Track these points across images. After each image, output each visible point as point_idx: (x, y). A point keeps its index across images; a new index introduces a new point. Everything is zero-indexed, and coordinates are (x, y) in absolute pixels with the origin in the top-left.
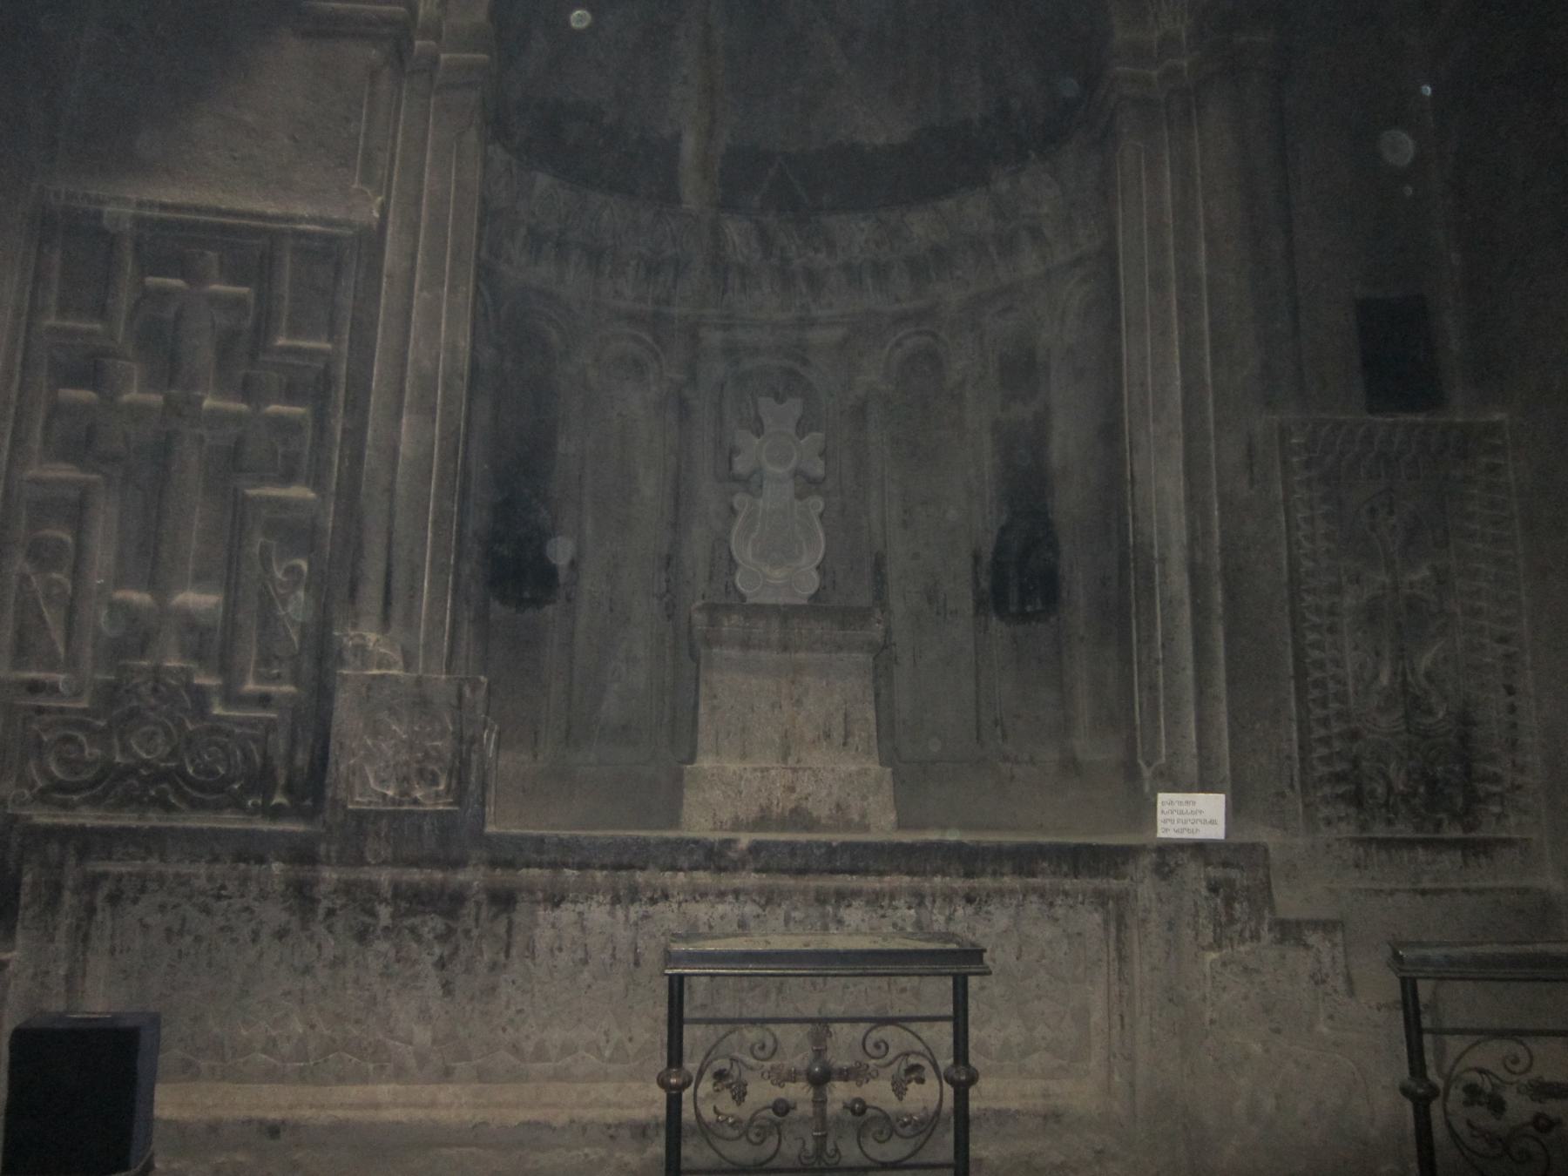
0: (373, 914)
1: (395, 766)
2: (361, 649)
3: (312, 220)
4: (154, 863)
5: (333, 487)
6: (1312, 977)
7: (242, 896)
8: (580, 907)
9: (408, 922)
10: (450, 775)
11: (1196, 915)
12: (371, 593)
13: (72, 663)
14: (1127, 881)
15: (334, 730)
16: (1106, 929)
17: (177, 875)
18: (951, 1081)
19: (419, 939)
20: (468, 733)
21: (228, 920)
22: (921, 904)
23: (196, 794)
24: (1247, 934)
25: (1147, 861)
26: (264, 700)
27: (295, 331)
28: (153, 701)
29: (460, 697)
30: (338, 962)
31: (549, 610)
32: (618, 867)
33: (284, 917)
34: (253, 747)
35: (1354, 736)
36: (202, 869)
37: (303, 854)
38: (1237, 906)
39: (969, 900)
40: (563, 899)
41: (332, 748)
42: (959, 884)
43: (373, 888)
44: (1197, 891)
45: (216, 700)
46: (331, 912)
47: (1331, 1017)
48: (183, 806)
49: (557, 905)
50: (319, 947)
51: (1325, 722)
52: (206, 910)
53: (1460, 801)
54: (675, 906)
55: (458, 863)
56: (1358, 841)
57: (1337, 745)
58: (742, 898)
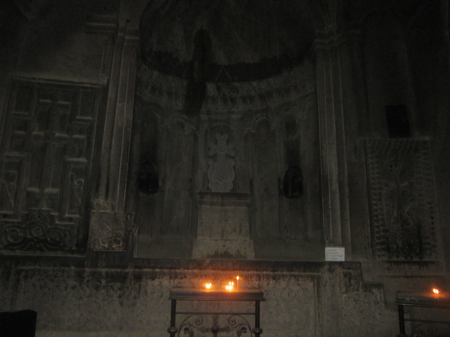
0: (100, 282)
1: (108, 238)
2: (98, 204)
3: (87, 83)
4: (37, 267)
5: (92, 159)
6: (374, 302)
7: (62, 276)
8: (160, 280)
9: (111, 284)
10: (123, 241)
11: (340, 284)
12: (103, 189)
14: (320, 274)
16: (314, 288)
18: (254, 333)
19: (113, 289)
22: (260, 280)
23: (50, 246)
24: (355, 289)
25: (326, 267)
26: (71, 219)
28: (39, 220)
29: (127, 219)
30: (90, 296)
31: (156, 194)
32: (171, 268)
33: (75, 283)
35: (387, 231)
36: (51, 268)
37: (80, 264)
38: (352, 281)
39: (274, 279)
40: (155, 278)
42: (271, 273)
43: (100, 274)
44: (340, 276)
45: (56, 219)
46: (88, 281)
47: (380, 314)
49: (153, 279)
50: (84, 291)
51: (378, 227)
52: (52, 281)
53: (418, 250)
54: (188, 280)
55: (125, 267)
56: (387, 262)
57: (382, 234)
58: (207, 277)
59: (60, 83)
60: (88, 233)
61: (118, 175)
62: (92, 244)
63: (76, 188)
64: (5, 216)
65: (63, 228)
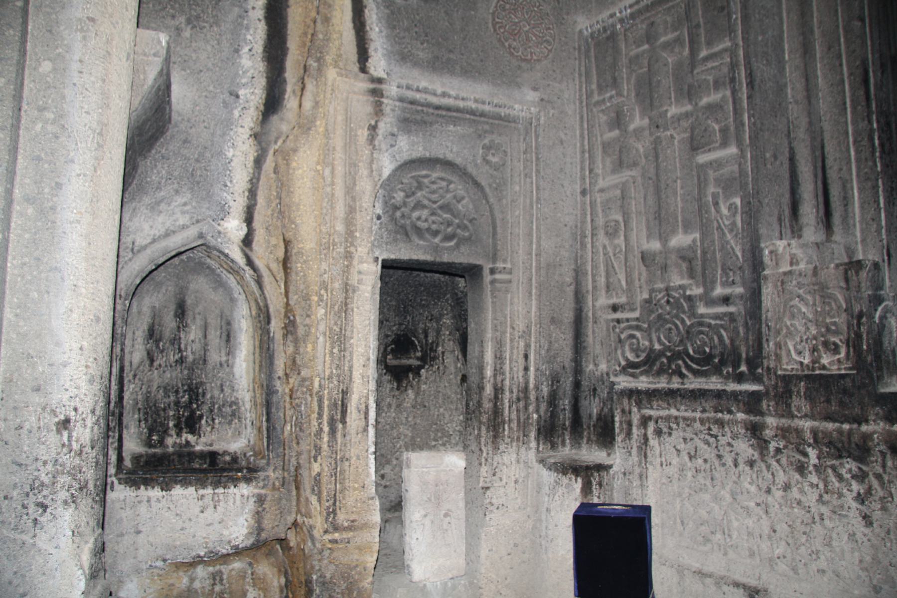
0: (805, 455)
1: (807, 339)
4: (673, 412)
5: (748, 141)
7: (723, 436)
10: (848, 346)
12: (809, 211)
13: (630, 290)
19: (840, 478)
20: (857, 309)
23: (694, 366)
26: (726, 300)
27: (709, 44)
28: (668, 308)
34: (723, 332)
36: (698, 415)
41: (763, 330)
43: (798, 432)
46: (778, 451)
48: (690, 375)
63: (727, 223)
64: (615, 308)
65: (713, 322)
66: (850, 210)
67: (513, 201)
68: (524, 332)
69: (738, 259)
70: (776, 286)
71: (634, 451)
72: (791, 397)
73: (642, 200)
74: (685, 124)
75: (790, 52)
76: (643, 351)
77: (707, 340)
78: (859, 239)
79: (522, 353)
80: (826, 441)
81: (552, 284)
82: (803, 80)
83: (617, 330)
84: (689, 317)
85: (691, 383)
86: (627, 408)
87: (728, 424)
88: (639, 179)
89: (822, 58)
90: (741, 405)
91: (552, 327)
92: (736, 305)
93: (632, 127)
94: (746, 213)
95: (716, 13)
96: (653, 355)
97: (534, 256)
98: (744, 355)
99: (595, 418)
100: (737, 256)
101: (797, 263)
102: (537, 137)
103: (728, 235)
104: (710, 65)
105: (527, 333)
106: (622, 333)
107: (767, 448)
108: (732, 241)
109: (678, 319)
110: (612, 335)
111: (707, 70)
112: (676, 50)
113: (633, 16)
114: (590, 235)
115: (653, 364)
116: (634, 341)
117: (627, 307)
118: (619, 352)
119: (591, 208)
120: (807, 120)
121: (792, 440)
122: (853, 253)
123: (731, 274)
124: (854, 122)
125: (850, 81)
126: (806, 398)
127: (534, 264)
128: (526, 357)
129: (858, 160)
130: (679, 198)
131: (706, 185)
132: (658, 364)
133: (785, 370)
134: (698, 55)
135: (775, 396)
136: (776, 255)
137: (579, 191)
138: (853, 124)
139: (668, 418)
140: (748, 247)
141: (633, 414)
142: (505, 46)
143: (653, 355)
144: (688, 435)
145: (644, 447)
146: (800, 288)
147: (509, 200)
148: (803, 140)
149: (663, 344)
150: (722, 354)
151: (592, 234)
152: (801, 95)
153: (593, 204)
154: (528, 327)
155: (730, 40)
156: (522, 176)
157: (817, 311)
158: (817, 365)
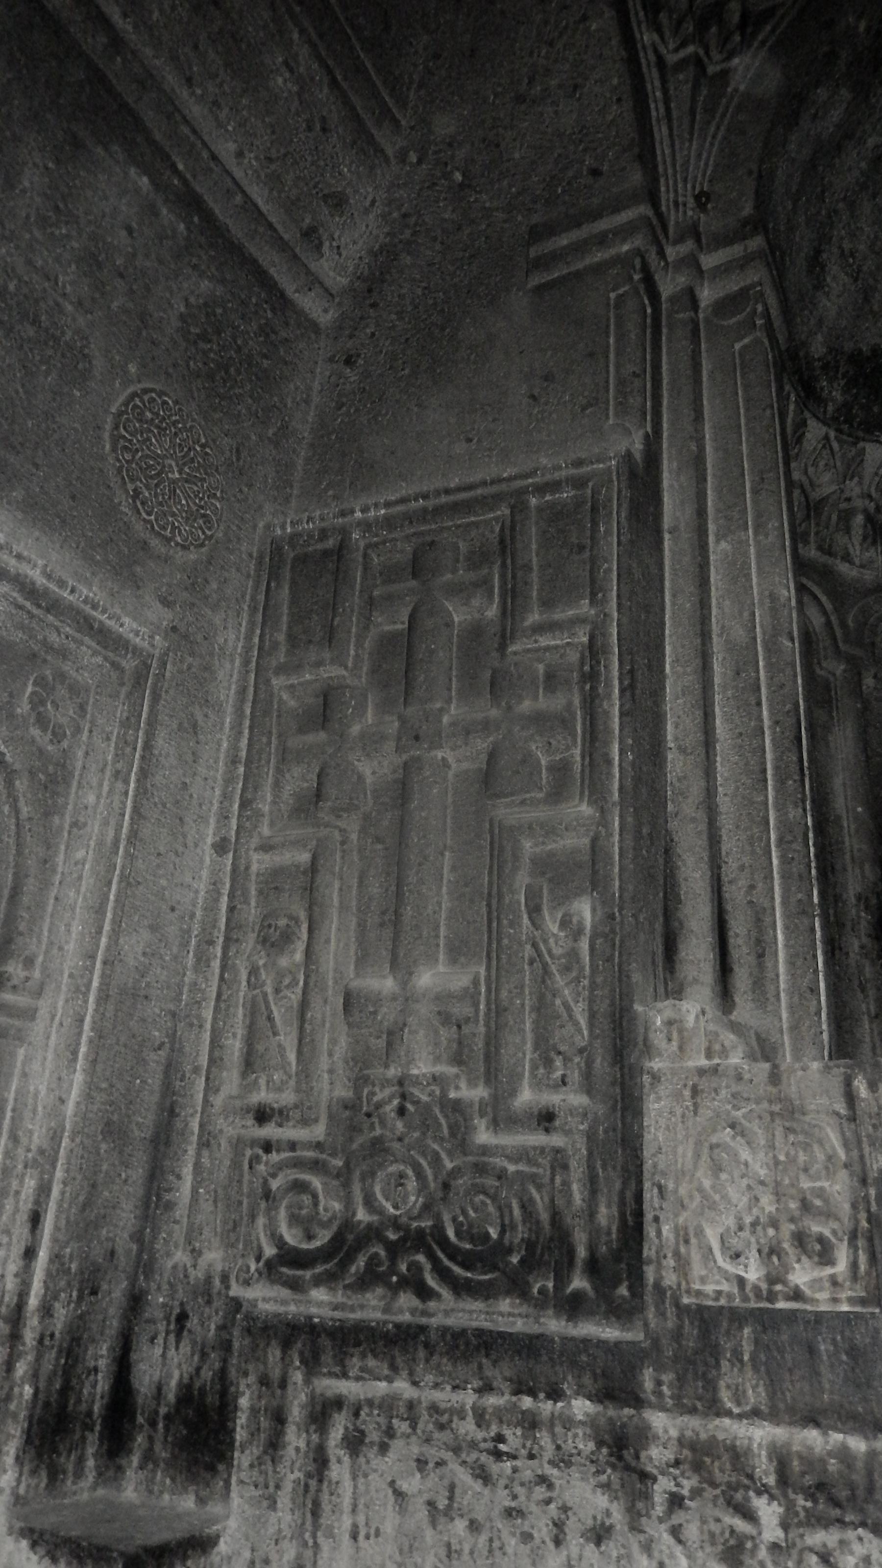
0: (750, 1515)
1: (754, 1224)
4: (402, 1387)
5: (616, 796)
7: (531, 1457)
9: (818, 1538)
12: (697, 953)
15: (648, 1165)
17: (434, 1408)
21: (515, 1497)
23: (457, 1270)
27: (547, 604)
29: (850, 1098)
33: (602, 1501)
36: (468, 1398)
41: (647, 1196)
43: (738, 1456)
46: (676, 1501)
48: (445, 1293)
52: (483, 1476)
59: (444, 499)
60: (639, 1197)
61: (769, 877)
62: (671, 1262)
63: (557, 951)
64: (262, 1115)
66: (769, 965)
67: (75, 824)
68: (41, 1152)
69: (580, 1031)
70: (677, 1096)
71: (284, 1499)
72: (718, 1365)
73: (355, 882)
74: (482, 744)
75: (676, 661)
76: (325, 1225)
77: (491, 1209)
78: (785, 1026)
79: (26, 1206)
80: (808, 1480)
81: (123, 1039)
82: (699, 713)
83: (262, 1168)
84: (450, 1154)
85: (447, 1313)
86: (276, 1374)
87: (552, 1425)
88: (354, 837)
89: (724, 687)
90: (587, 1380)
91: (104, 1146)
92: (567, 1133)
93: (355, 729)
94: (606, 936)
95: (565, 552)
96: (350, 1237)
97: (98, 965)
98: (582, 1252)
99: (171, 1397)
100: (576, 1024)
101: (724, 1052)
102: (156, 698)
103: (558, 977)
104: (545, 641)
105: (47, 1158)
106: (274, 1176)
107: (647, 1496)
108: (566, 992)
109: (424, 1154)
110: (246, 1177)
111: (537, 650)
112: (476, 602)
113: (389, 523)
114: (221, 939)
115: (349, 1258)
116: (306, 1199)
117: (296, 1114)
118: (261, 1221)
119: (233, 880)
120: (703, 783)
121: (719, 1477)
122: (774, 1049)
123: (558, 1062)
124: (780, 808)
125: (774, 733)
126: (756, 1369)
127: (95, 984)
128: (35, 1219)
129: (784, 877)
130: (444, 889)
131: (515, 869)
132: (361, 1262)
133: (699, 1293)
134: (523, 619)
135: (676, 1359)
136: (680, 1031)
137: (209, 840)
138: (778, 810)
139: (387, 1405)
140: (603, 1007)
141: (290, 1388)
142: (127, 491)
143: (350, 1237)
144: (433, 1453)
145: (313, 1483)
146: (736, 1108)
147: (68, 820)
148: (693, 820)
149: (381, 1212)
150: (530, 1245)
151: (228, 939)
152: (695, 737)
153: (238, 874)
154: (55, 1137)
155: (592, 602)
156: (108, 773)
157: (777, 1163)
158: (779, 1287)
